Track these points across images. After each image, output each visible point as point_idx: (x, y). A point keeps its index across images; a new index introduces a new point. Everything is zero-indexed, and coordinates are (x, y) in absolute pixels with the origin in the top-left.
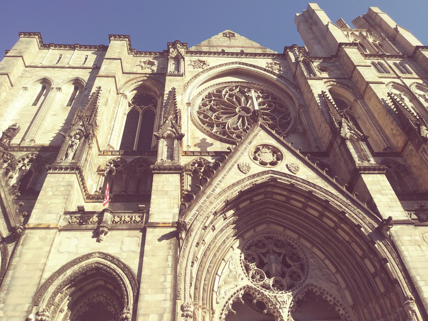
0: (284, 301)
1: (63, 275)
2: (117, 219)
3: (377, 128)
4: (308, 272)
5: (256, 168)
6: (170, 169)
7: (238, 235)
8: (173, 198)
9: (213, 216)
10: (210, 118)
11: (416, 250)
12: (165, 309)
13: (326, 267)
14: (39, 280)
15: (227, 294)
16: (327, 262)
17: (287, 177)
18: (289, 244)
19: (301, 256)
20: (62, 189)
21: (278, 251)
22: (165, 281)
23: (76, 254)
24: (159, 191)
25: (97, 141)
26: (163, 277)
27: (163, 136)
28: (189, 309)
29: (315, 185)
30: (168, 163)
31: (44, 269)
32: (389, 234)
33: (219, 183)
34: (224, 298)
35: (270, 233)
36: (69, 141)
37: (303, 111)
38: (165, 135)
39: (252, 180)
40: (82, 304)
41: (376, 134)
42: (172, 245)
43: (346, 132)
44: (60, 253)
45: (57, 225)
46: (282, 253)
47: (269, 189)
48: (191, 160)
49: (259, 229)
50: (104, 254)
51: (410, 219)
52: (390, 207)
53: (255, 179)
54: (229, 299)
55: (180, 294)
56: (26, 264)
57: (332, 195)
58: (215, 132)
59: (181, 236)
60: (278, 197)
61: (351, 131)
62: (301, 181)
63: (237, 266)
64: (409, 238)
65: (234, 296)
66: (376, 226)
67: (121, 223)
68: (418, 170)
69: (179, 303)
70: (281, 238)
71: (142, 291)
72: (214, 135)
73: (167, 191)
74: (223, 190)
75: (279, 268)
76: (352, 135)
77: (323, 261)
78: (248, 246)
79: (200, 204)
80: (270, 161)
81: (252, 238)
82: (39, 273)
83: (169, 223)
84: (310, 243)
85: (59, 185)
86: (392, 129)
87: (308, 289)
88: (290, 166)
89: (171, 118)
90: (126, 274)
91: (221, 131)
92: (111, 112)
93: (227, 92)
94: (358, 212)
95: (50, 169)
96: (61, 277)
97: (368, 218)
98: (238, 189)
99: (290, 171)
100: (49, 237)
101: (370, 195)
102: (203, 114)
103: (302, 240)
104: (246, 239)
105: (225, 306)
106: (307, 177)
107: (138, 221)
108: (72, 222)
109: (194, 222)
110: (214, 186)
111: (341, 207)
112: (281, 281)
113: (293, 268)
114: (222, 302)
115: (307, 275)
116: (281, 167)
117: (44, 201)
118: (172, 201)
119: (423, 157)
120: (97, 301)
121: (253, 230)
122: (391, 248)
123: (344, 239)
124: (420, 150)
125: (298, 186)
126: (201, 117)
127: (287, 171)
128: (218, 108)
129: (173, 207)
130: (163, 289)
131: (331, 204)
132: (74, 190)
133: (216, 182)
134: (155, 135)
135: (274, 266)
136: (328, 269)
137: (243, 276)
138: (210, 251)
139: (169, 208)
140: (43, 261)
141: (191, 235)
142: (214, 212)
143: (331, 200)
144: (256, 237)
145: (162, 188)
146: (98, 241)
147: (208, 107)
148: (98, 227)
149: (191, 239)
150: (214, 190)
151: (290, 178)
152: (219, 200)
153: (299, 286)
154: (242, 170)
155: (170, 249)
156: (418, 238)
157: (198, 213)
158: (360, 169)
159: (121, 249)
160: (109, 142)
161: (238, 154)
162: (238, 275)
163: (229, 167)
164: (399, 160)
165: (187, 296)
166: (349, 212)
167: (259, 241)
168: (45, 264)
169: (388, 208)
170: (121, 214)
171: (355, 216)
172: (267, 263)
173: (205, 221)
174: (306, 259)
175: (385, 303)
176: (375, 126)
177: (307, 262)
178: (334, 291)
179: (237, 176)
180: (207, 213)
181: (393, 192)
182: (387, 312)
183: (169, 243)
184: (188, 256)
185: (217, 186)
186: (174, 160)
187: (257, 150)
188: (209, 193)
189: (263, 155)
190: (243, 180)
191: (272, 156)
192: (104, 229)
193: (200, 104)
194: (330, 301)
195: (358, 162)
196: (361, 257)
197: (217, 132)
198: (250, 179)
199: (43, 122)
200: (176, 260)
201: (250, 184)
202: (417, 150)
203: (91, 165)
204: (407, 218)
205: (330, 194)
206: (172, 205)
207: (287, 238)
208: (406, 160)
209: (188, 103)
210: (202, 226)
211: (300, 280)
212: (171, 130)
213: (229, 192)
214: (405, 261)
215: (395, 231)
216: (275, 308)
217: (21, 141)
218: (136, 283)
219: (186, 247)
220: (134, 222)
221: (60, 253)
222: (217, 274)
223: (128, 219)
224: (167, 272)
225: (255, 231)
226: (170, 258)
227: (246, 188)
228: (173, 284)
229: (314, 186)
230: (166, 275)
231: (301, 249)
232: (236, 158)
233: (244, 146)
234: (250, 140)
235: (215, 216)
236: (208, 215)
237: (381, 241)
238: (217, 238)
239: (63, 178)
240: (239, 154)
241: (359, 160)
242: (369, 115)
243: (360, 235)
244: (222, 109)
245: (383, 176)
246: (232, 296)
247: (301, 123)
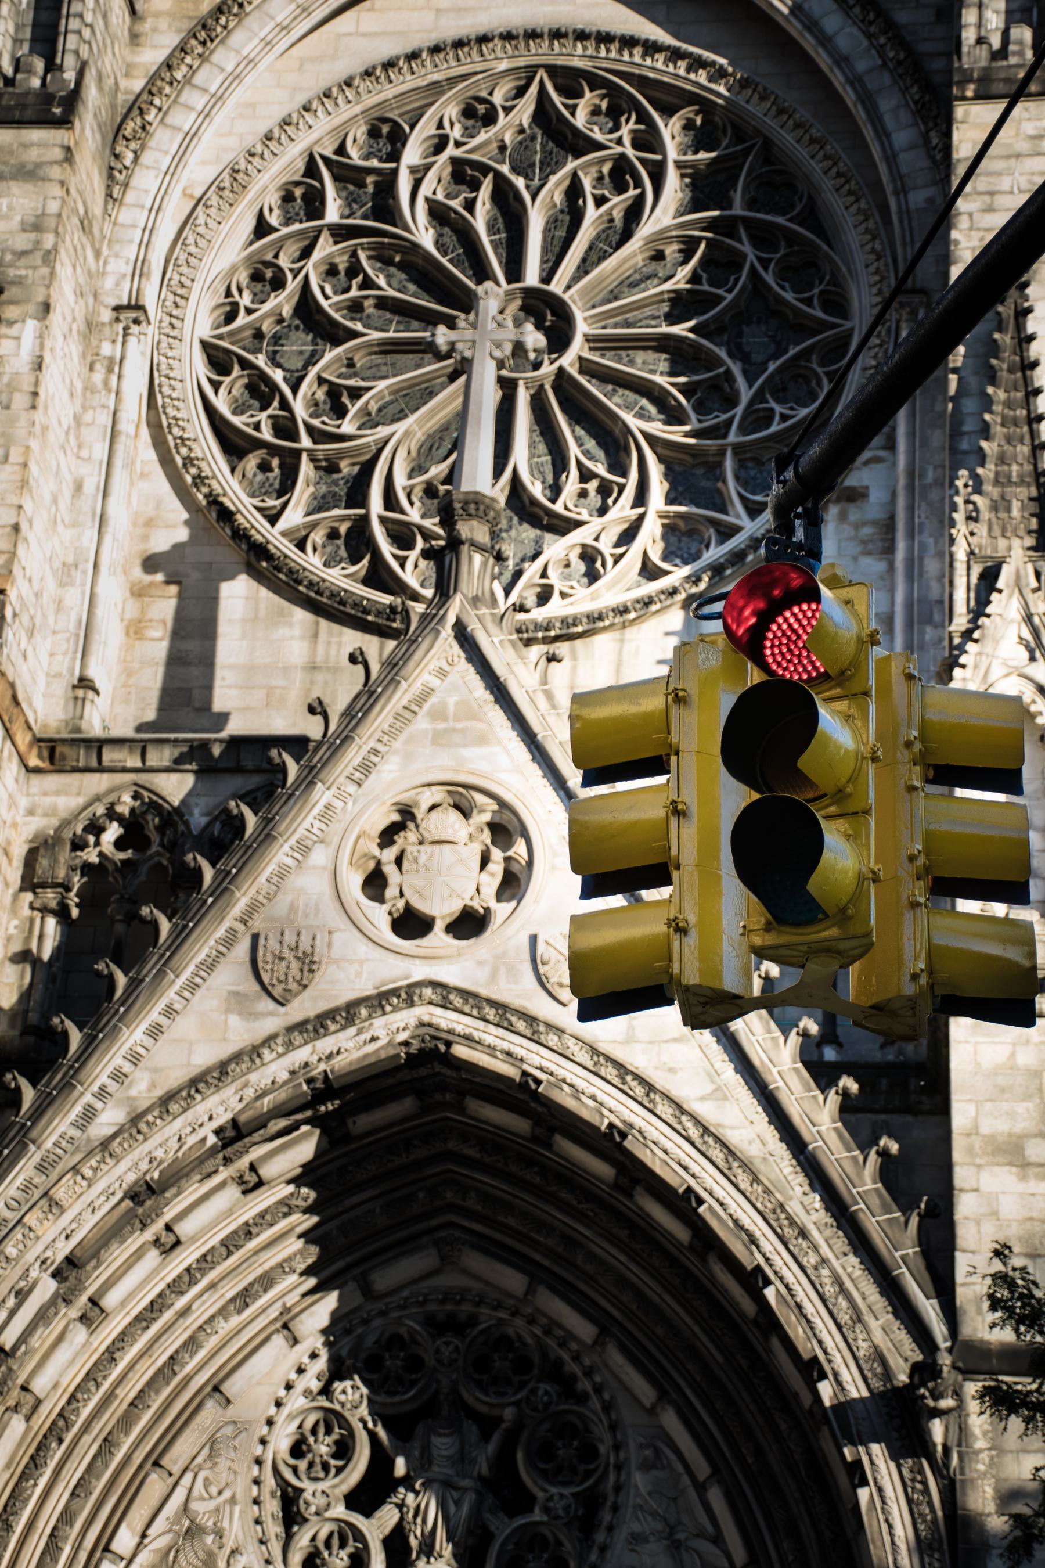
7: (325, 1274)
13: (710, 1528)
17: (510, 1029)
18: (555, 1373)
19: (602, 1449)
21: (483, 1409)
29: (650, 1088)
39: (308, 1048)
48: (81, 801)
53: (326, 1044)
62: (584, 1057)
63: (233, 1501)
77: (701, 1488)
93: (440, 144)
113: (537, 1516)
136: (718, 1539)
142: (60, 1257)
144: (377, 1323)
150: (89, 1114)
151: (529, 1034)
152: (100, 1186)
154: (266, 979)
162: (227, 1551)
163: (202, 956)
167: (395, 1342)
177: (618, 1488)
179: (234, 1020)
180: (19, 1271)
193: (233, 270)
201: (293, 1073)
205: (718, 1155)
207: (548, 1332)
231: (607, 1407)
232: (252, 891)
234: (372, 744)
236: (22, 1284)
238: (117, 1355)
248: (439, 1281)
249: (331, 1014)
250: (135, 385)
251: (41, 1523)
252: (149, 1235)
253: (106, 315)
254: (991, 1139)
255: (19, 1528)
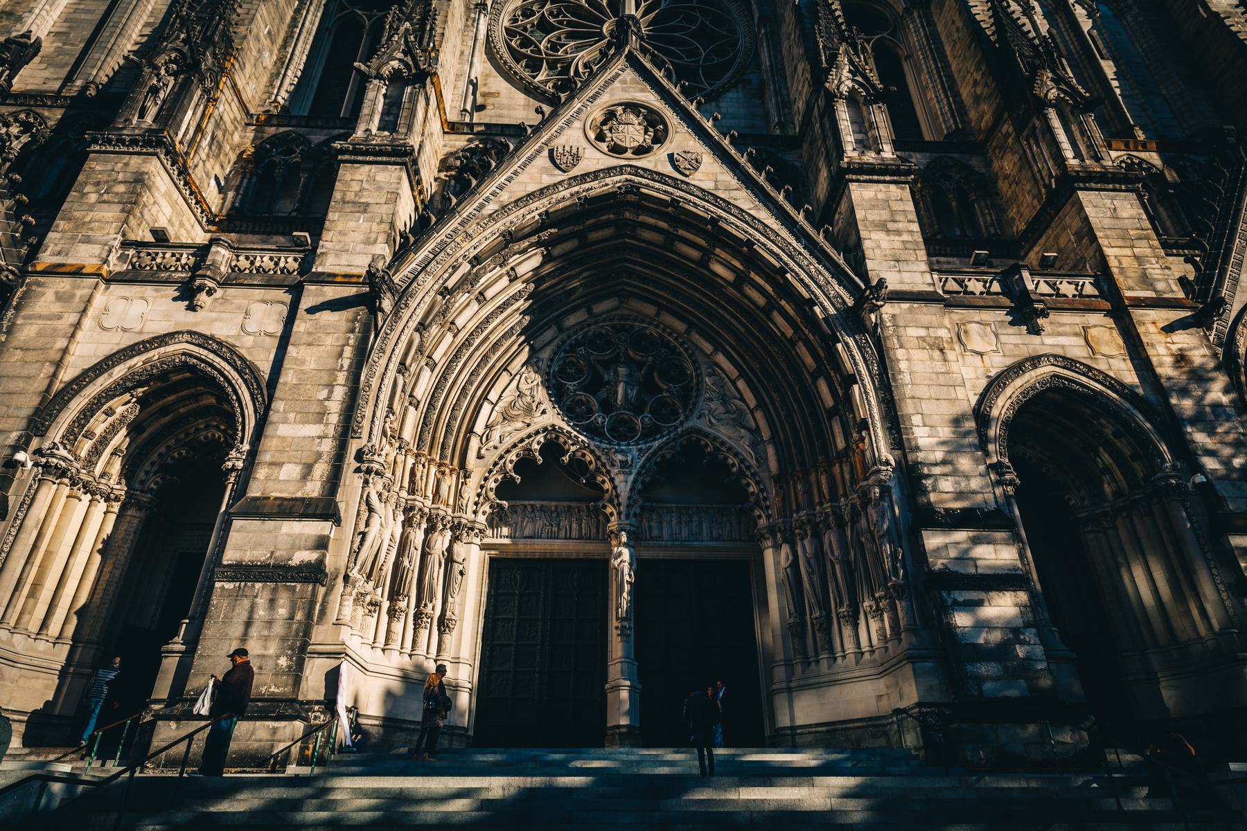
0: (627, 461)
1: (106, 375)
2: (243, 263)
3: (942, 82)
4: (694, 404)
5: (594, 159)
6: (381, 153)
8: (378, 220)
9: (469, 266)
10: (536, 46)
11: (932, 358)
12: (319, 455)
13: (738, 396)
14: (47, 382)
15: (506, 440)
16: (741, 384)
17: (666, 183)
20: (121, 188)
22: (328, 399)
23: (141, 333)
24: (348, 202)
25: (234, 86)
26: (326, 391)
27: (378, 73)
28: (376, 457)
29: (729, 203)
30: (381, 138)
31: (61, 360)
32: (874, 320)
33: (498, 191)
34: (496, 448)
35: (626, 320)
36: (150, 78)
37: (766, 33)
38: (386, 71)
40: (172, 442)
41: (936, 97)
42: (357, 325)
43: (843, 79)
44: (104, 329)
45: (99, 268)
46: (645, 363)
47: (627, 215)
49: (599, 308)
50: (200, 335)
51: (940, 292)
52: (898, 261)
53: (587, 186)
54: (508, 451)
55: (359, 428)
56: (21, 349)
57: (765, 229)
58: (541, 82)
59: (380, 303)
60: (647, 235)
61: (854, 75)
64: (922, 332)
65: (520, 445)
66: (850, 302)
67: (251, 272)
68: (1010, 185)
69: (354, 446)
70: (653, 331)
71: (273, 417)
72: (538, 88)
73: (367, 204)
74: (503, 208)
75: (633, 394)
76: (856, 87)
77: (734, 383)
78: (571, 345)
79: (443, 237)
80: (636, 144)
81: (582, 329)
82: (49, 369)
83: (359, 276)
84: (710, 343)
85: (115, 181)
86: (976, 83)
87: (689, 440)
88: (679, 158)
89: (407, 30)
90: (245, 381)
91: (558, 80)
92: (288, 20)
94: (817, 269)
95: (95, 141)
96: (100, 380)
97: (836, 287)
98: (540, 205)
99: (676, 168)
100: (79, 293)
101: (858, 231)
102: (521, 35)
103: (696, 337)
104: (568, 329)
105: (495, 464)
106: (716, 185)
107: (291, 270)
108: (140, 266)
109: (420, 278)
110: (484, 197)
111: (778, 258)
112: (632, 421)
114: (492, 457)
115: (692, 411)
116: (657, 161)
117: (77, 214)
118: (375, 227)
119: (1028, 151)
120: (206, 437)
121: (584, 310)
122: (873, 353)
123: (783, 334)
124: (1025, 133)
125: (687, 206)
126: (513, 43)
127: (668, 169)
128: (559, 22)
129: (375, 241)
130: (321, 416)
131: (758, 249)
132: (157, 195)
133: (489, 189)
134: (358, 70)
135: (620, 389)
136: (742, 399)
137: (547, 405)
138: (472, 349)
139: (365, 244)
140: (61, 343)
141: (406, 305)
142: (471, 256)
143: (758, 241)
144: (593, 327)
145: (356, 196)
146: (192, 308)
147: (535, 19)
148: (193, 278)
149: (406, 314)
150: (482, 206)
152: (489, 230)
153: (669, 433)
154: (558, 162)
155: (352, 331)
156: (943, 333)
157: (432, 256)
158: (851, 169)
159: (242, 328)
160: (277, 95)
161: (560, 122)
162: (536, 403)
164: (976, 163)
165: (375, 432)
166: (797, 269)
167: (599, 335)
168: (65, 351)
169: (893, 263)
170: (253, 253)
171: (807, 280)
172: (609, 383)
173: (446, 275)
174: (697, 376)
175: (842, 472)
176: (940, 77)
178: (744, 448)
179: (544, 177)
180: (453, 260)
181: (916, 227)
182: (841, 492)
183: (350, 318)
184: (393, 350)
185: (491, 197)
186: (397, 132)
187: (610, 115)
188: (467, 213)
189: (620, 129)
190: (555, 185)
191: (642, 132)
192: (206, 282)
194: (734, 465)
195: (851, 152)
196: (811, 374)
197: (547, 81)
198: (574, 184)
199: (119, 40)
200: (362, 355)
201: (572, 195)
202: (1019, 131)
203: (220, 147)
204: (931, 289)
206: (373, 236)
207: (664, 330)
208: (989, 164)
209: (481, 4)
210: (436, 287)
211: (676, 420)
212: (400, 60)
213: (517, 213)
214: (895, 380)
215: (894, 316)
216: (608, 472)
217: (63, 86)
218: (264, 400)
219: (392, 330)
220: (282, 272)
221: (104, 329)
222: (486, 398)
223: (267, 263)
224: (336, 380)
225: (590, 312)
226: (348, 352)
227: (561, 205)
228: (345, 405)
229: (727, 205)
230: (333, 386)
231: (691, 356)
233: (577, 105)
235: (473, 266)
237: (852, 335)
239: (126, 164)
240: (560, 124)
241: (854, 149)
242: (931, 49)
243: (811, 320)
244: (570, 24)
245: (903, 189)
246: (515, 446)
247: (758, 66)
248: (618, 312)
249: (588, 174)
250: (482, 36)
251: (459, 382)
252: (504, 271)
253: (472, 7)
254: (873, 221)
255: (451, 381)
